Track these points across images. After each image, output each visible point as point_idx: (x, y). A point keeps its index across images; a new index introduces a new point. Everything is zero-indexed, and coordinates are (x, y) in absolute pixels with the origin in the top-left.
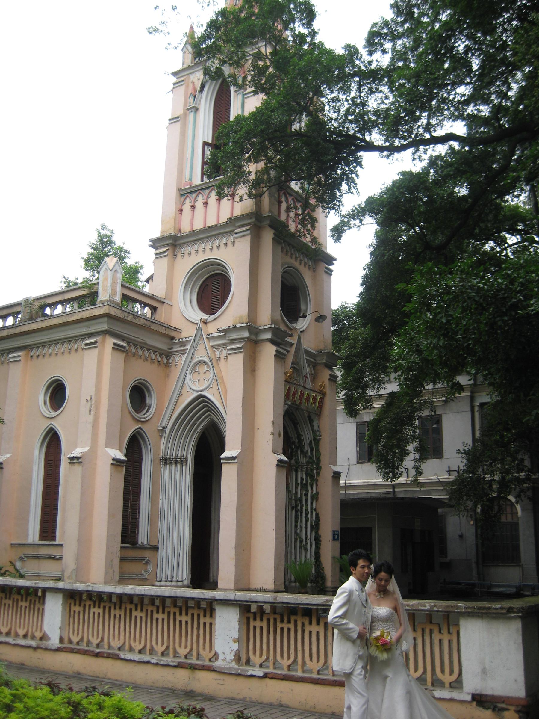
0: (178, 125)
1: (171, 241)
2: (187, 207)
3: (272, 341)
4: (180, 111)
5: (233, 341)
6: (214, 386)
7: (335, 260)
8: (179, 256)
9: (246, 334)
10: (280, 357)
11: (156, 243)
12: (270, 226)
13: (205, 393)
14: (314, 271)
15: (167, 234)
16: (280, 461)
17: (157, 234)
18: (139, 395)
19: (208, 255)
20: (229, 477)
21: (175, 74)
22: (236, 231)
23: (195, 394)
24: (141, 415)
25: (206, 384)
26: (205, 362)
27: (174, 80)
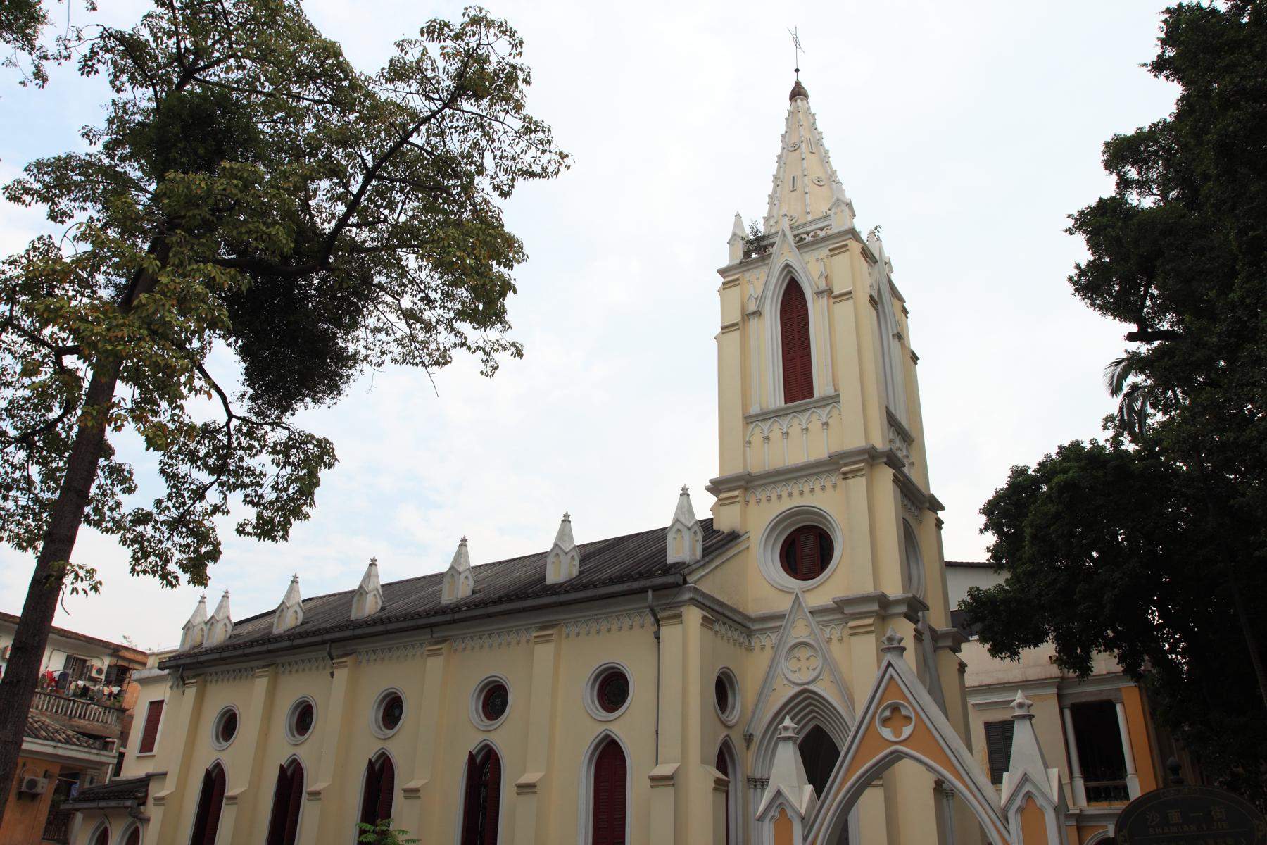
0: (735, 336)
1: (742, 483)
2: (757, 439)
3: (908, 616)
4: (736, 317)
6: (825, 676)
8: (752, 501)
9: (875, 607)
11: (715, 487)
15: (729, 473)
17: (715, 475)
18: (723, 688)
19: (797, 501)
21: (722, 272)
22: (844, 469)
23: (797, 689)
24: (724, 717)
25: (815, 674)
27: (720, 280)
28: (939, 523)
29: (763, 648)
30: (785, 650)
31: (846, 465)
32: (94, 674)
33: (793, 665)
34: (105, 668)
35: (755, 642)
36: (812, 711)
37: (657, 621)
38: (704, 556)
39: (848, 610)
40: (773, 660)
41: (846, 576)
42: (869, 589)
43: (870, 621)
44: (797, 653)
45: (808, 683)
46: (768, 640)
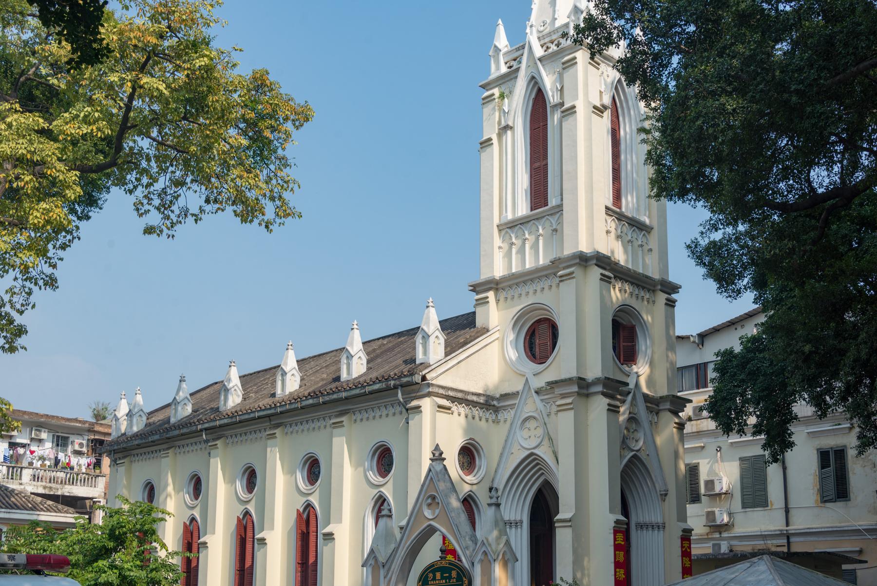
3: (605, 394)
5: (564, 396)
6: (546, 442)
7: (680, 287)
9: (575, 388)
10: (613, 410)
12: (596, 265)
13: (535, 451)
14: (654, 302)
16: (617, 522)
20: (563, 538)
22: (560, 273)
23: (527, 452)
25: (537, 441)
26: (535, 418)
28: (671, 304)
29: (505, 421)
30: (520, 422)
31: (564, 268)
32: (77, 448)
33: (525, 433)
34: (85, 442)
35: (501, 416)
36: (540, 469)
37: (407, 410)
38: (447, 354)
39: (558, 391)
40: (509, 431)
41: (563, 364)
42: (573, 374)
43: (569, 400)
44: (527, 424)
45: (534, 448)
46: (508, 415)
